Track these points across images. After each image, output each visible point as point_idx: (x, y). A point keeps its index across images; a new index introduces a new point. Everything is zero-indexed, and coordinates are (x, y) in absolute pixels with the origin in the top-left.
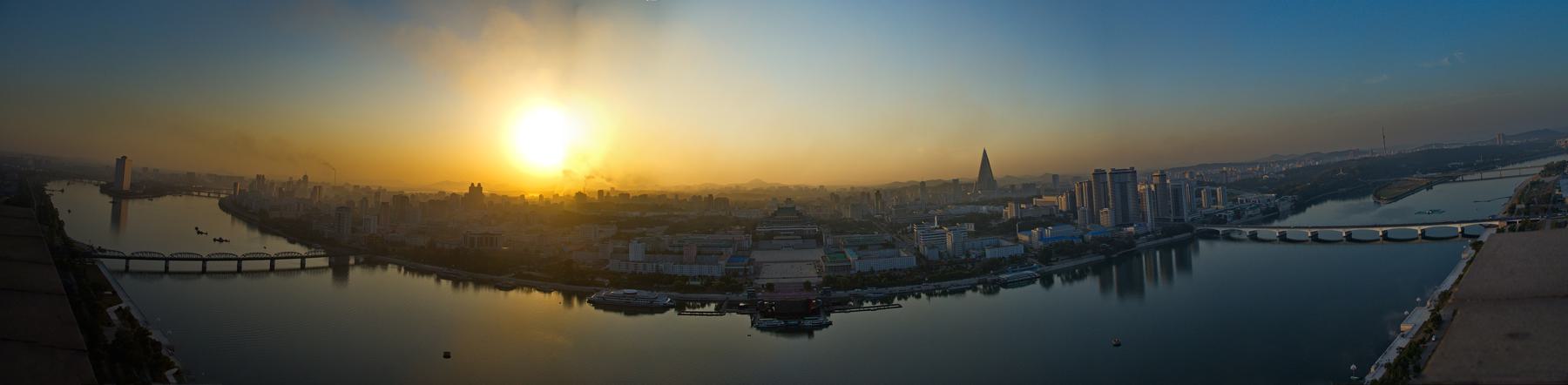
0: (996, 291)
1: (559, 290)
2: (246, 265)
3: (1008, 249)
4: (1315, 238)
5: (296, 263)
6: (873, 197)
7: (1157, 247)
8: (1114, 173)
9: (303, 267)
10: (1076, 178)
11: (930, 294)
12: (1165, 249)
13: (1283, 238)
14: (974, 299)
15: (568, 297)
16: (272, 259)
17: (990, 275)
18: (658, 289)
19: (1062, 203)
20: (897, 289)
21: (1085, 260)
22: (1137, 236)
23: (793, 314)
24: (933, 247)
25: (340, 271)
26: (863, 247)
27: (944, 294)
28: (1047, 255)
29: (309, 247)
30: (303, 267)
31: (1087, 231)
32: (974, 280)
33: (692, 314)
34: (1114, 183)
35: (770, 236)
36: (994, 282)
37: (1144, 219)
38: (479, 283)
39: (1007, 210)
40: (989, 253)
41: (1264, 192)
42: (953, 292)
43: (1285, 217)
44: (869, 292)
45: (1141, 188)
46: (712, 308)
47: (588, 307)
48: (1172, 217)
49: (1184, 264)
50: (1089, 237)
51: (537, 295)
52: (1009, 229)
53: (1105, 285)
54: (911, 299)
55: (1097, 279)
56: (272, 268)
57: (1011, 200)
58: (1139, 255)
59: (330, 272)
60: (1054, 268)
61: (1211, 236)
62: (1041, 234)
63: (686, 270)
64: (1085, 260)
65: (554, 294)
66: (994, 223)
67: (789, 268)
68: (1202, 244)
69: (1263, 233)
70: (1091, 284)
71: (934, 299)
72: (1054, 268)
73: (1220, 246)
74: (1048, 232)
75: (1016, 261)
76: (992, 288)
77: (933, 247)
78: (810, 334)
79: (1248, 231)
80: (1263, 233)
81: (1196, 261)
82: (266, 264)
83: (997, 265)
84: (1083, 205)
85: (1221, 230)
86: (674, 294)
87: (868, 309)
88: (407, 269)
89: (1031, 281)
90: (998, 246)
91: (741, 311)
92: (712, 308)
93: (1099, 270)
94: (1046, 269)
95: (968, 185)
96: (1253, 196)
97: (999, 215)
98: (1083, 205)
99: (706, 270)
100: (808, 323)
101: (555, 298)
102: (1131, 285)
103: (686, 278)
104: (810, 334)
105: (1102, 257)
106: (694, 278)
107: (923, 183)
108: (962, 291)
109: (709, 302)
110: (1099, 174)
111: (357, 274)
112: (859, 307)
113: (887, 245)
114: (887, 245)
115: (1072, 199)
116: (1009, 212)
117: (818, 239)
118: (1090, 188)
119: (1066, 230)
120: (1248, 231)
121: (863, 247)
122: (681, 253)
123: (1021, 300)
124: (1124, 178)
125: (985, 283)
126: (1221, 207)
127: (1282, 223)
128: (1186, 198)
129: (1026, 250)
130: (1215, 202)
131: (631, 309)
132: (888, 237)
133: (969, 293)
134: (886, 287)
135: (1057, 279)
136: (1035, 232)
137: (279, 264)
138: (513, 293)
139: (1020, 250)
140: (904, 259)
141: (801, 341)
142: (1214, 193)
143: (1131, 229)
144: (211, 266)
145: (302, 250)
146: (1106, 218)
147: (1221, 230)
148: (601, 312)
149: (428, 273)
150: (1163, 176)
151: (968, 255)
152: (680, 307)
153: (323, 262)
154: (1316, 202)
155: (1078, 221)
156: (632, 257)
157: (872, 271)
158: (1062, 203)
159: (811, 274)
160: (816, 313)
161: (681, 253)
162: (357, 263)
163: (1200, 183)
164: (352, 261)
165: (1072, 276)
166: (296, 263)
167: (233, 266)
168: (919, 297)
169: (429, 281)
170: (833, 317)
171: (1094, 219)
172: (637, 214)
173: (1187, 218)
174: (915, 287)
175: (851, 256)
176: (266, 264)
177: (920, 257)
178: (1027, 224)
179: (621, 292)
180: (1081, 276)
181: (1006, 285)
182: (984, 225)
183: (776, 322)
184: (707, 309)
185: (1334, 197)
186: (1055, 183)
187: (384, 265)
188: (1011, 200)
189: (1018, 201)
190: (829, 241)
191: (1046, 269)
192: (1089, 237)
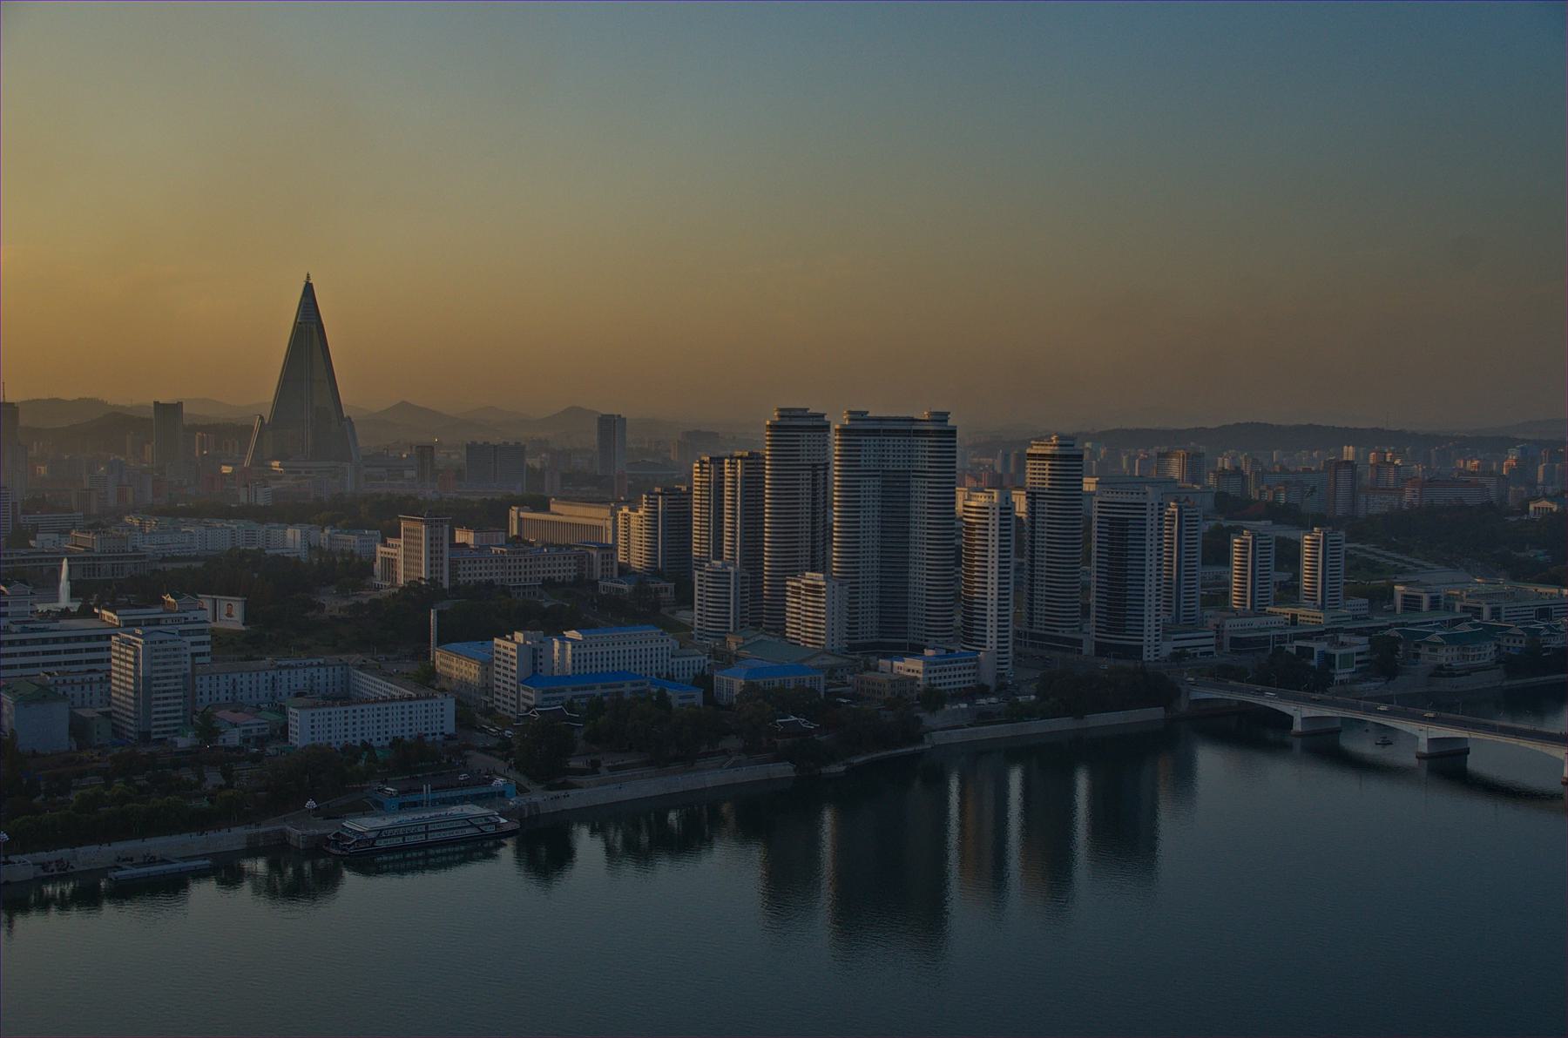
0: (327, 881)
3: (385, 707)
7: (1016, 752)
8: (862, 430)
10: (695, 438)
12: (1050, 765)
14: (223, 920)
19: (632, 534)
21: (710, 777)
22: (933, 699)
24: (45, 695)
27: (88, 898)
28: (546, 749)
31: (724, 659)
32: (232, 838)
34: (862, 475)
36: (317, 848)
37: (970, 632)
39: (396, 549)
40: (306, 728)
41: (1523, 572)
42: (124, 892)
45: (970, 501)
48: (1090, 634)
49: (1127, 836)
50: (732, 682)
52: (399, 629)
53: (785, 885)
55: (756, 854)
57: (413, 508)
58: (937, 780)
60: (575, 799)
61: (1255, 733)
62: (534, 658)
64: (710, 777)
66: (332, 603)
68: (1210, 762)
69: (1492, 752)
70: (727, 875)
72: (575, 799)
73: (1286, 782)
74: (563, 650)
75: (416, 764)
76: (306, 874)
77: (45, 695)
79: (1423, 734)
80: (1492, 752)
81: (1173, 830)
83: (334, 776)
84: (716, 549)
85: (1300, 712)
89: (478, 846)
90: (344, 696)
93: (762, 818)
94: (540, 798)
95: (227, 433)
96: (1468, 587)
97: (361, 569)
98: (716, 549)
102: (892, 894)
108: (172, 885)
110: (796, 428)
116: (404, 557)
118: (752, 484)
119: (638, 649)
120: (1423, 734)
124: (904, 457)
125: (276, 851)
126: (1309, 614)
128: (1160, 559)
129: (465, 719)
130: (1289, 591)
133: (204, 893)
135: (588, 847)
136: (510, 646)
139: (439, 717)
142: (1288, 555)
143: (911, 666)
146: (811, 610)
147: (1300, 712)
150: (1068, 460)
151: (209, 730)
155: (692, 617)
158: (632, 534)
163: (1233, 506)
165: (651, 836)
171: (761, 610)
173: (1155, 646)
178: (477, 613)
181: (370, 858)
182: (290, 607)
186: (608, 454)
188: (413, 508)
189: (442, 516)
192: (732, 682)
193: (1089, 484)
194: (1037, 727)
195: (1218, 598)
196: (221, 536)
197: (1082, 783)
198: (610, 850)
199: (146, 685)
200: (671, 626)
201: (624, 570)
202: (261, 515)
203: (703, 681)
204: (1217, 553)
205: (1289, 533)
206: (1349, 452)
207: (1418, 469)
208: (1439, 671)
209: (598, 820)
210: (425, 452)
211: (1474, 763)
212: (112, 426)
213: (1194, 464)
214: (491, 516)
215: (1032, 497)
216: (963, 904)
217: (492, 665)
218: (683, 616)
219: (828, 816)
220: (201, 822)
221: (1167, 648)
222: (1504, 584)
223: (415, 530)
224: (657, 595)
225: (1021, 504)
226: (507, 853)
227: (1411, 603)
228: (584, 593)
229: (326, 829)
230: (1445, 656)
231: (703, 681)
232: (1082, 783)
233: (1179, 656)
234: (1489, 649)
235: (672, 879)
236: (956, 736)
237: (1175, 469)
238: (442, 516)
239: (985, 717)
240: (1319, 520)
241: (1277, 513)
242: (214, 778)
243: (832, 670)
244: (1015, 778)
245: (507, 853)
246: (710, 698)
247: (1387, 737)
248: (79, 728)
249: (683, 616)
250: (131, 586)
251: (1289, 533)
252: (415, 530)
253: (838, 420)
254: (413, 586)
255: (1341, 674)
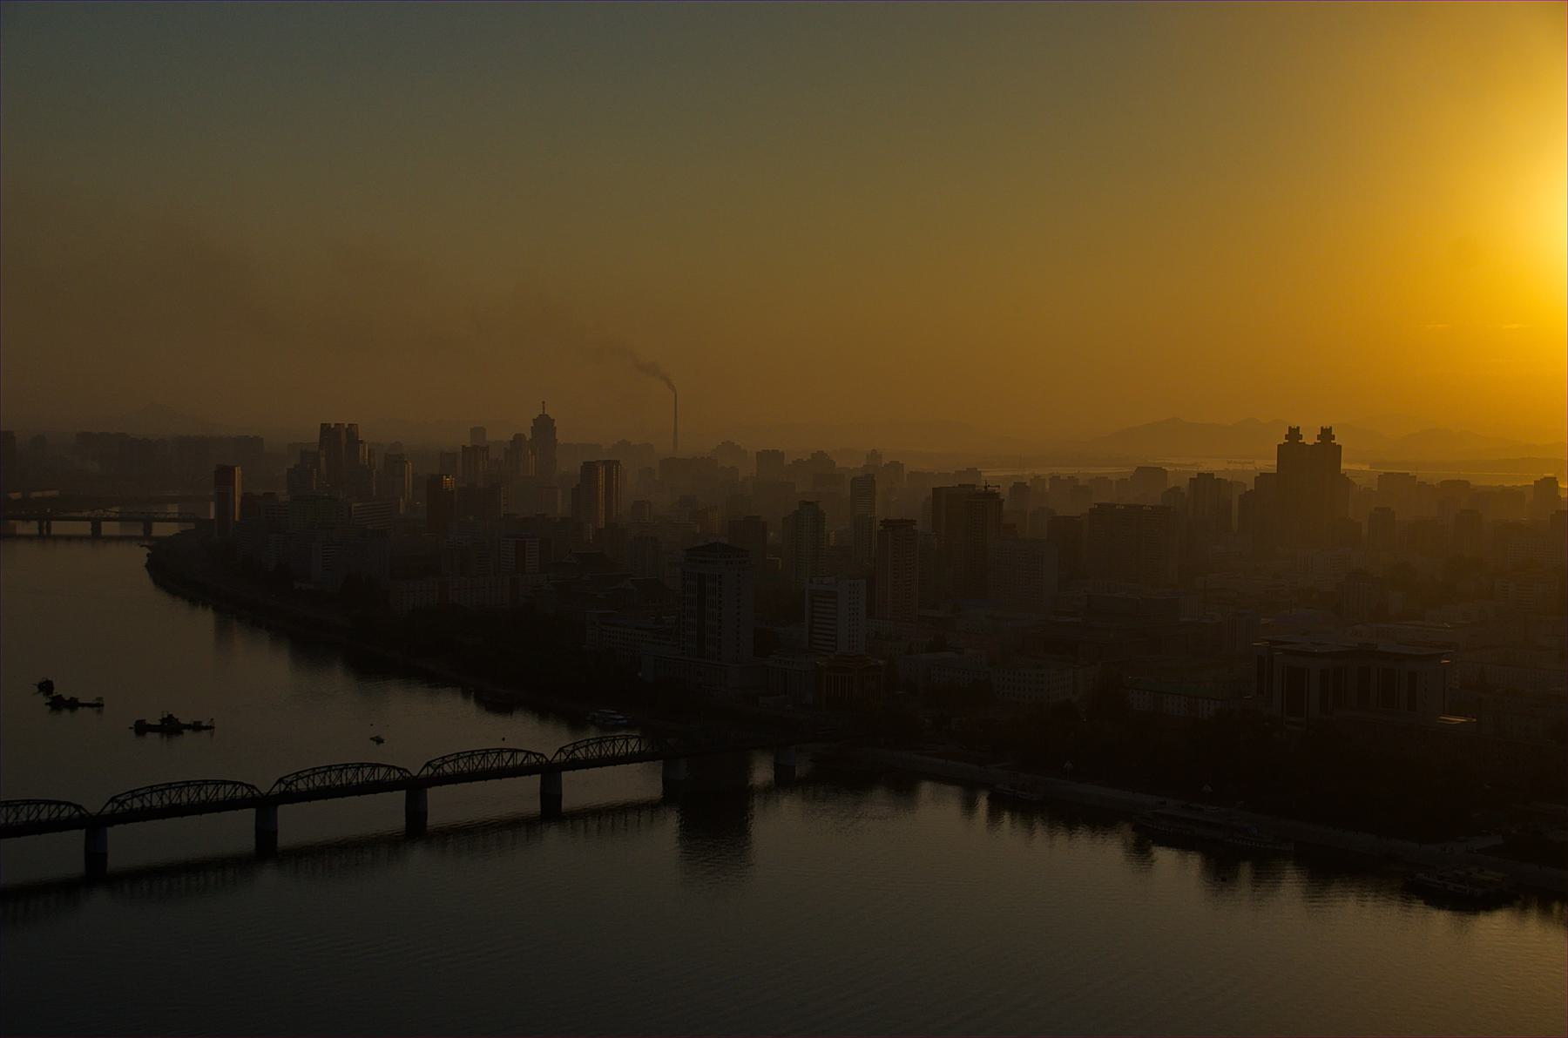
2: (296, 825)
5: (524, 794)
9: (552, 810)
16: (415, 788)
25: (712, 817)
29: (575, 722)
30: (552, 810)
38: (1329, 869)
56: (417, 827)
59: (670, 825)
82: (388, 811)
88: (998, 805)
111: (784, 829)
137: (444, 805)
144: (128, 846)
145: (539, 737)
149: (1097, 819)
153: (637, 782)
162: (784, 782)
164: (762, 773)
166: (524, 794)
167: (238, 831)
169: (1097, 859)
176: (388, 811)
187: (903, 786)
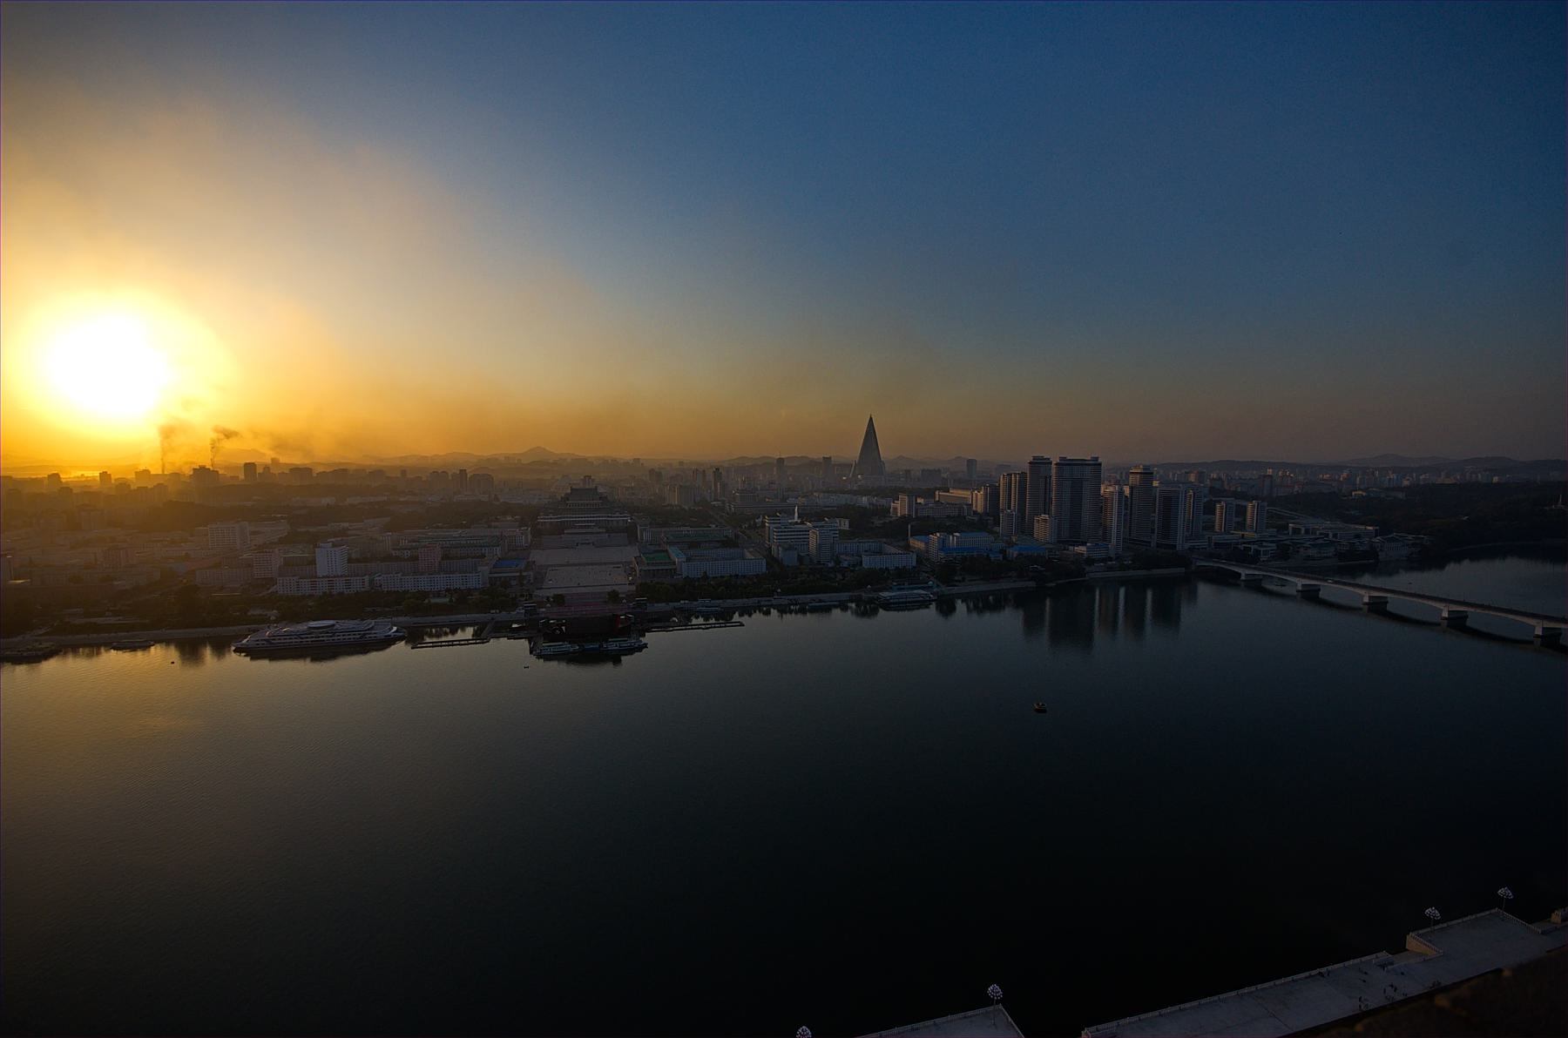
0: (874, 612)
1: (167, 641)
3: (894, 557)
4: (1457, 623)
6: (710, 477)
8: (1064, 464)
11: (783, 610)
13: (1377, 608)
14: (842, 620)
15: (190, 651)
17: (865, 590)
18: (375, 615)
19: (978, 500)
20: (740, 602)
21: (1004, 585)
22: (1090, 561)
23: (589, 636)
24: (790, 548)
26: (694, 545)
27: (803, 611)
28: (948, 571)
31: (1011, 544)
32: (845, 596)
33: (434, 645)
35: (559, 529)
36: (871, 601)
37: (1105, 537)
39: (898, 504)
40: (868, 562)
42: (813, 610)
43: (1390, 570)
44: (699, 604)
45: (1106, 489)
46: (470, 632)
47: (234, 660)
49: (1167, 615)
51: (113, 660)
52: (899, 530)
53: (1031, 624)
54: (757, 616)
55: (1020, 614)
60: (955, 590)
61: (1225, 579)
62: (943, 542)
63: (424, 583)
64: (1004, 585)
65: (156, 652)
66: (877, 522)
67: (591, 573)
68: (1204, 590)
70: (1009, 621)
71: (787, 617)
72: (955, 590)
73: (1237, 600)
74: (953, 539)
75: (903, 576)
76: (868, 609)
77: (790, 548)
78: (617, 661)
79: (1300, 582)
80: (1331, 590)
81: (1187, 615)
83: (878, 578)
86: (401, 619)
87: (698, 627)
89: (923, 604)
90: (880, 553)
91: (514, 634)
92: (470, 632)
93: (1021, 600)
94: (945, 589)
97: (885, 511)
99: (457, 581)
100: (613, 645)
101: (159, 658)
102: (1072, 630)
103: (425, 595)
104: (617, 661)
105: (1032, 584)
106: (438, 594)
107: (781, 460)
108: (827, 609)
109: (463, 626)
110: (1039, 464)
112: (685, 623)
113: (727, 543)
114: (727, 543)
115: (993, 496)
116: (900, 507)
117: (631, 533)
119: (980, 540)
120: (1300, 582)
121: (694, 545)
122: (415, 558)
123: (908, 630)
124: (1079, 475)
125: (858, 601)
126: (1249, 534)
127: (1379, 582)
129: (919, 561)
130: (1241, 526)
131: (322, 651)
132: (729, 532)
133: (837, 612)
134: (724, 598)
135: (961, 606)
138: (51, 666)
139: (911, 560)
140: (750, 562)
141: (607, 670)
142: (1242, 511)
143: (1082, 549)
146: (1043, 528)
147: (1244, 572)
148: (264, 664)
150: (1147, 474)
151: (838, 562)
152: (414, 637)
154: (1475, 556)
155: (999, 530)
156: (322, 569)
157: (705, 577)
158: (978, 500)
159: (621, 582)
160: (625, 632)
161: (415, 558)
163: (1217, 492)
165: (983, 604)
168: (768, 613)
170: (649, 638)
171: (1025, 528)
172: (326, 501)
173: (1181, 544)
174: (764, 601)
175: (677, 555)
177: (772, 561)
178: (924, 526)
179: (303, 627)
180: (997, 606)
181: (888, 606)
182: (864, 523)
183: (566, 646)
184: (460, 635)
185: (1525, 552)
186: (970, 475)
188: (903, 490)
189: (913, 493)
190: (647, 536)
191: (945, 589)
192: (1013, 553)
193: (1155, 484)
194: (1131, 573)
195: (1209, 527)
196: (843, 499)
197: (1149, 595)
198: (969, 610)
199: (819, 547)
200: (991, 532)
201: (975, 513)
202: (855, 493)
203: (1003, 552)
204: (1210, 509)
205: (1243, 503)
206: (1270, 472)
207: (1301, 478)
208: (1308, 558)
209: (965, 598)
210: (908, 472)
211: (1322, 595)
212: (812, 464)
213: (1201, 476)
214: (929, 494)
215: (1132, 489)
216: (1099, 635)
217: (930, 544)
218: (996, 529)
219: (1048, 602)
220: (837, 590)
221: (1187, 545)
222: (1340, 524)
223: (904, 498)
224: (986, 522)
225: (1127, 491)
226: (933, 606)
227: (1296, 531)
228: (959, 520)
229: (874, 595)
230: (1311, 552)
231: (1003, 552)
232: (1149, 595)
233: (1192, 549)
234: (1331, 551)
235: (989, 618)
236: (1099, 575)
237: (1192, 478)
238: (913, 493)
239: (1110, 569)
240: (1255, 498)
241: (1236, 495)
242: (840, 576)
243: (1051, 550)
244: (1122, 591)
245: (933, 606)
246: (1005, 558)
247: (1284, 583)
248: (800, 559)
249: (996, 529)
250: (815, 515)
251: (1243, 503)
252: (904, 498)
253: (1055, 460)
254: (903, 517)
255: (1263, 558)
